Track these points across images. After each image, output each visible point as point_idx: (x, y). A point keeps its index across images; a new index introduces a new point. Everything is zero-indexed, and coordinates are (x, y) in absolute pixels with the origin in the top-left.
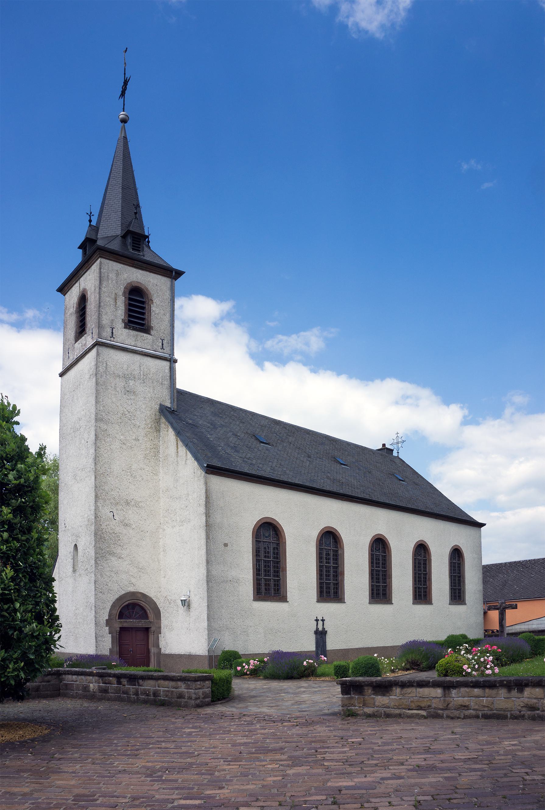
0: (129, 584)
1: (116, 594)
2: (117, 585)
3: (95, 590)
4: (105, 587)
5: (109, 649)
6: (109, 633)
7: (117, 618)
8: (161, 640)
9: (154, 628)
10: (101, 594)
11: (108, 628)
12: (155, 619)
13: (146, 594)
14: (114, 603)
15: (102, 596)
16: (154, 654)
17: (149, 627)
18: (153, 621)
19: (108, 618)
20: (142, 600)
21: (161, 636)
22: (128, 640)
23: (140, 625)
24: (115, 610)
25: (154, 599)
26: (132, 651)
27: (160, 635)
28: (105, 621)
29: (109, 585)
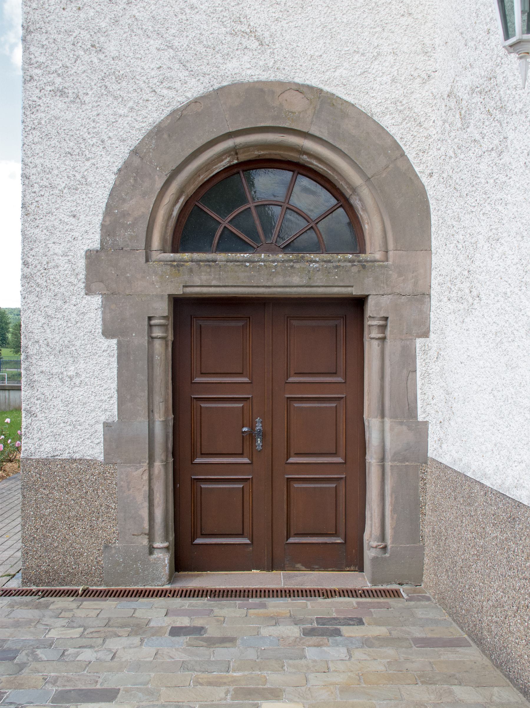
0: (234, 34)
1: (152, 97)
2: (155, 43)
3: (28, 79)
4: (86, 58)
5: (107, 425)
6: (107, 333)
7: (156, 243)
8: (427, 375)
9: (385, 301)
10: (60, 104)
11: (96, 300)
12: (391, 246)
13: (340, 92)
14: (135, 152)
15: (69, 115)
16: (383, 459)
17: (367, 294)
18: (378, 256)
19: (96, 245)
20: (314, 130)
21: (425, 352)
22: (240, 374)
23: (296, 280)
24: (144, 195)
25: (386, 122)
26: (263, 435)
27: (419, 342)
28: (82, 263)
29: (112, 48)
